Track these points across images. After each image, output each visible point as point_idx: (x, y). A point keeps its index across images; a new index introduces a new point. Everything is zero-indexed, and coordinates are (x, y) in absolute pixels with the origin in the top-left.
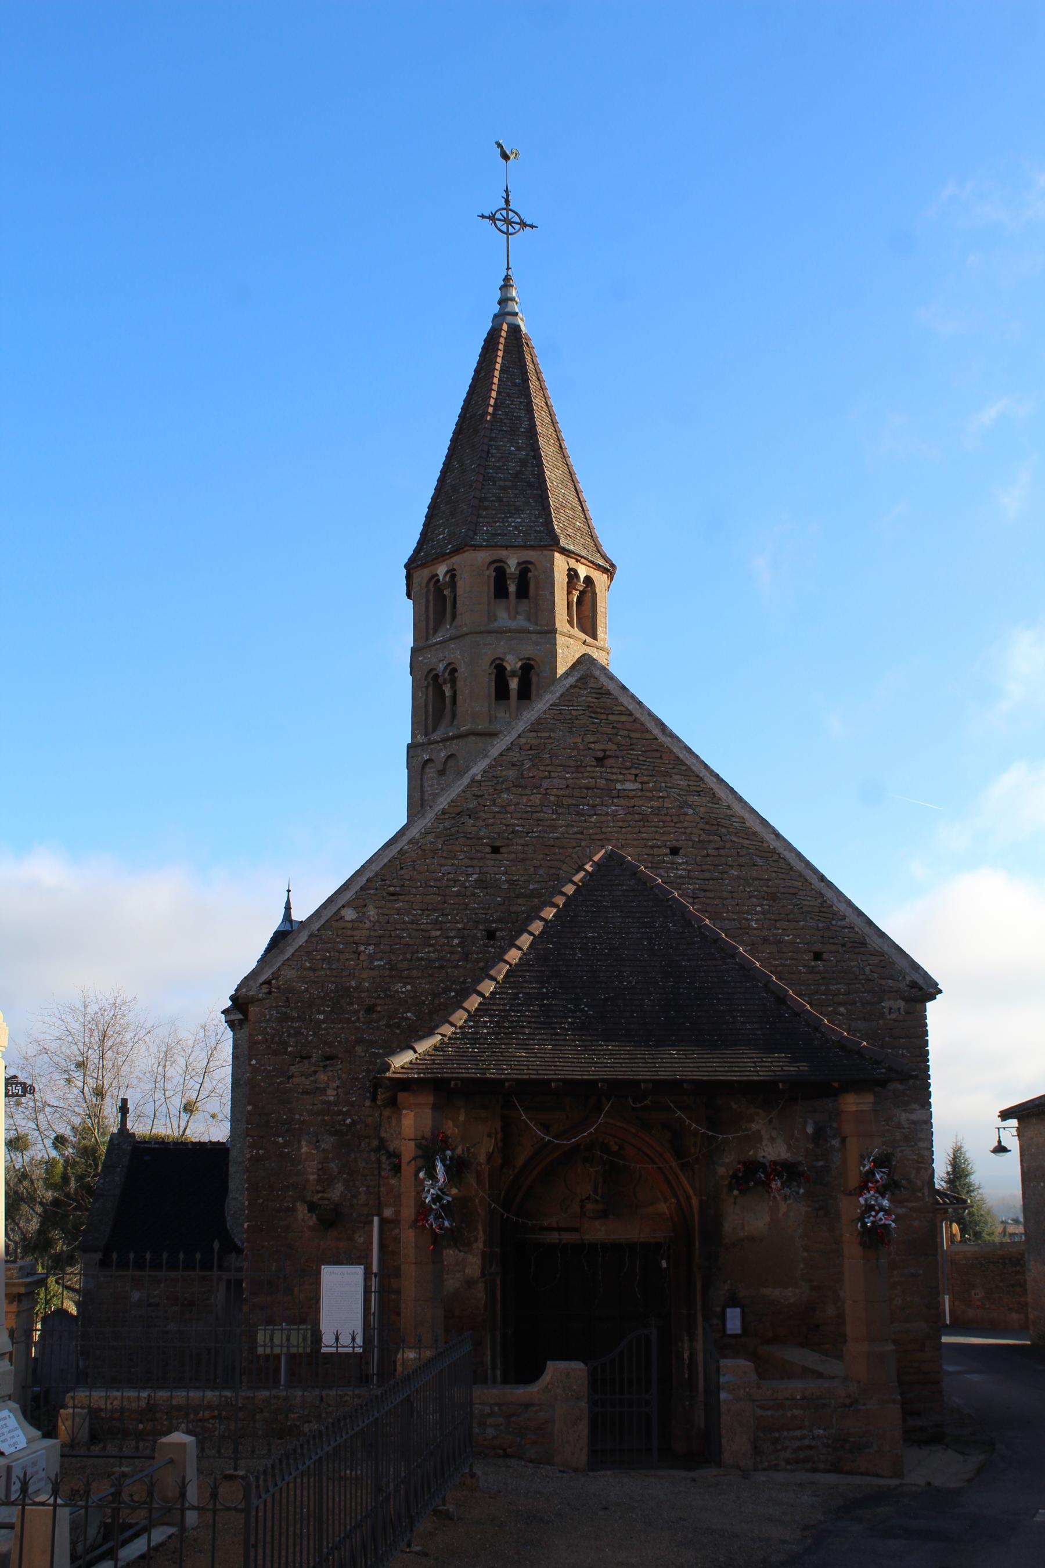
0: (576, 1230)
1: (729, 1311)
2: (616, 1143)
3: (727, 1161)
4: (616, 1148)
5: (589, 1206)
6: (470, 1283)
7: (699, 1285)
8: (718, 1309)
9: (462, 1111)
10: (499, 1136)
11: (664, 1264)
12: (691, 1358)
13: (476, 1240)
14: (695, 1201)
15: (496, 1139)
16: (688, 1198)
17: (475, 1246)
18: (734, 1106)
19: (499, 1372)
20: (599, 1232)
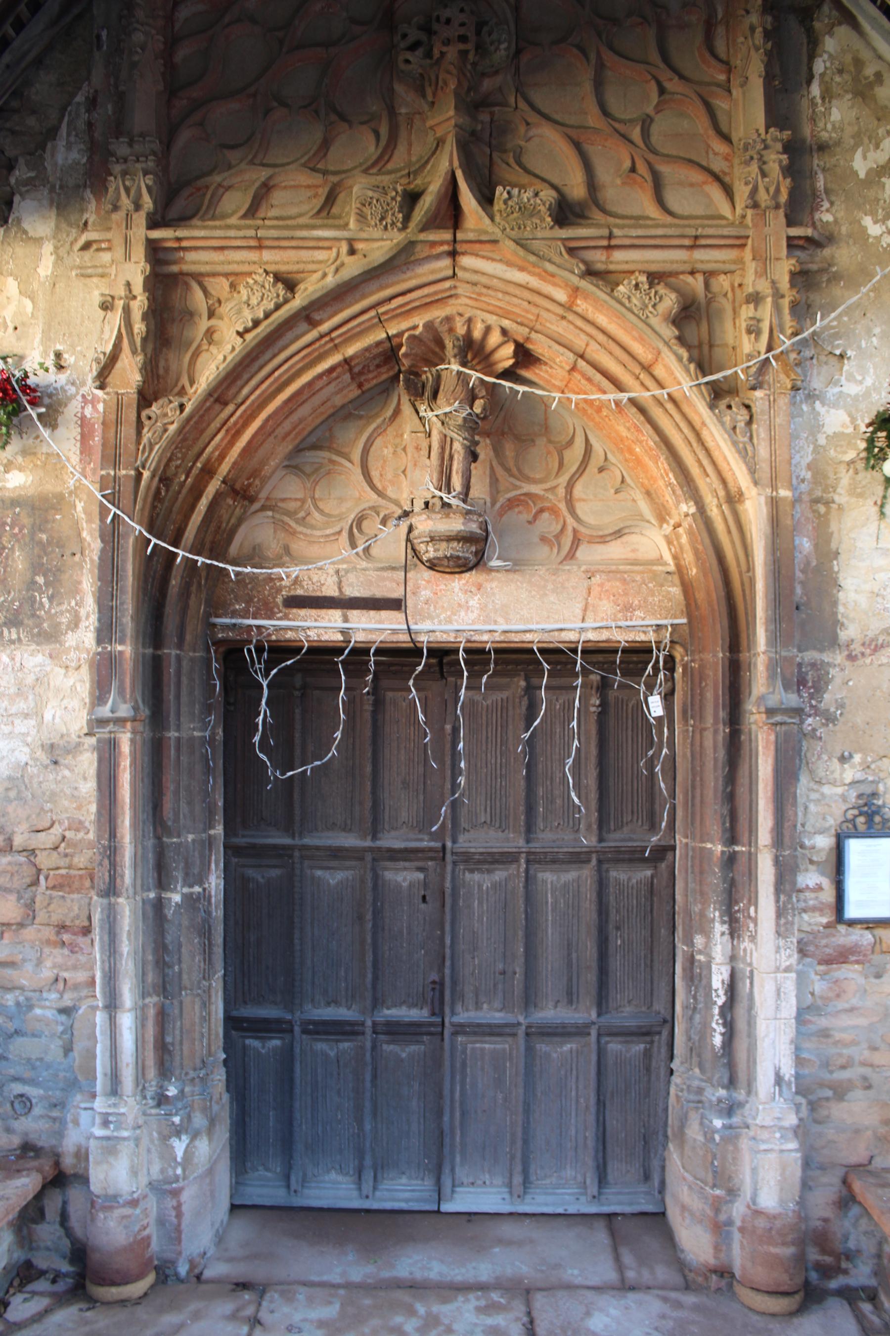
0: (396, 604)
1: (855, 848)
2: (504, 332)
3: (852, 389)
4: (505, 356)
5: (424, 524)
6: (56, 753)
7: (765, 768)
8: (824, 842)
9: (48, 248)
10: (140, 305)
11: (656, 706)
12: (732, 988)
13: (75, 624)
14: (755, 511)
15: (127, 310)
16: (733, 499)
17: (71, 639)
18: (874, 229)
19: (127, 1021)
20: (459, 612)
